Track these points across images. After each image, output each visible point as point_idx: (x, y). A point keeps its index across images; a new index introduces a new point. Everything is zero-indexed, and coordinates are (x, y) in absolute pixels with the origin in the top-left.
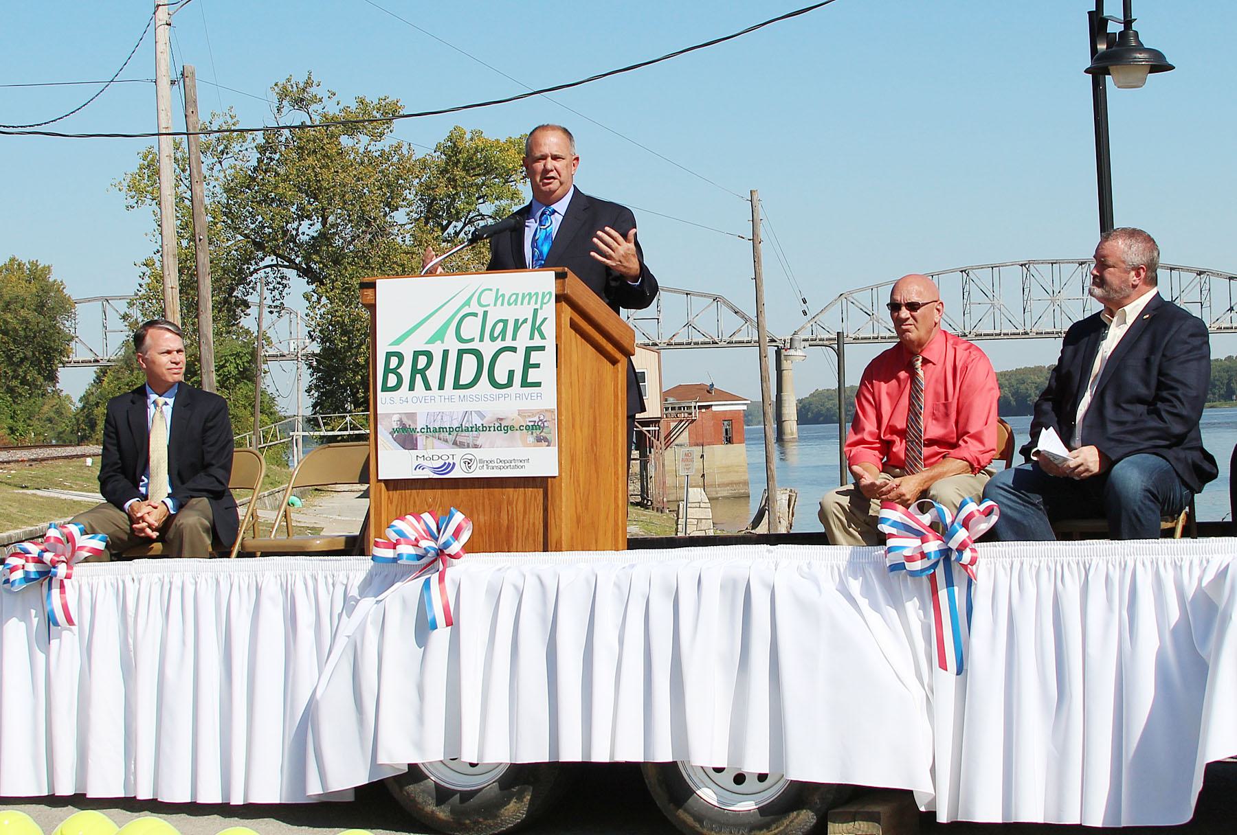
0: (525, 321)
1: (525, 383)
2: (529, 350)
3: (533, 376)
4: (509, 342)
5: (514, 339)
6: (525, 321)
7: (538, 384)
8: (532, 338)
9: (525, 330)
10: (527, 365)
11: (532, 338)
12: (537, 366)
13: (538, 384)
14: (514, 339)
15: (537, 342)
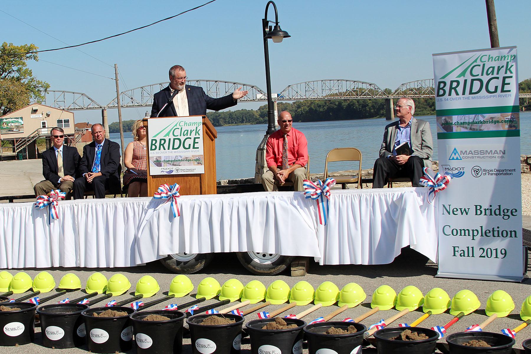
0: (503, 67)
1: (503, 91)
2: (504, 78)
3: (506, 88)
4: (495, 75)
5: (498, 74)
6: (503, 67)
7: (509, 91)
8: (506, 73)
9: (503, 70)
10: (504, 84)
11: (506, 73)
12: (509, 84)
13: (509, 91)
14: (498, 74)
15: (508, 74)
